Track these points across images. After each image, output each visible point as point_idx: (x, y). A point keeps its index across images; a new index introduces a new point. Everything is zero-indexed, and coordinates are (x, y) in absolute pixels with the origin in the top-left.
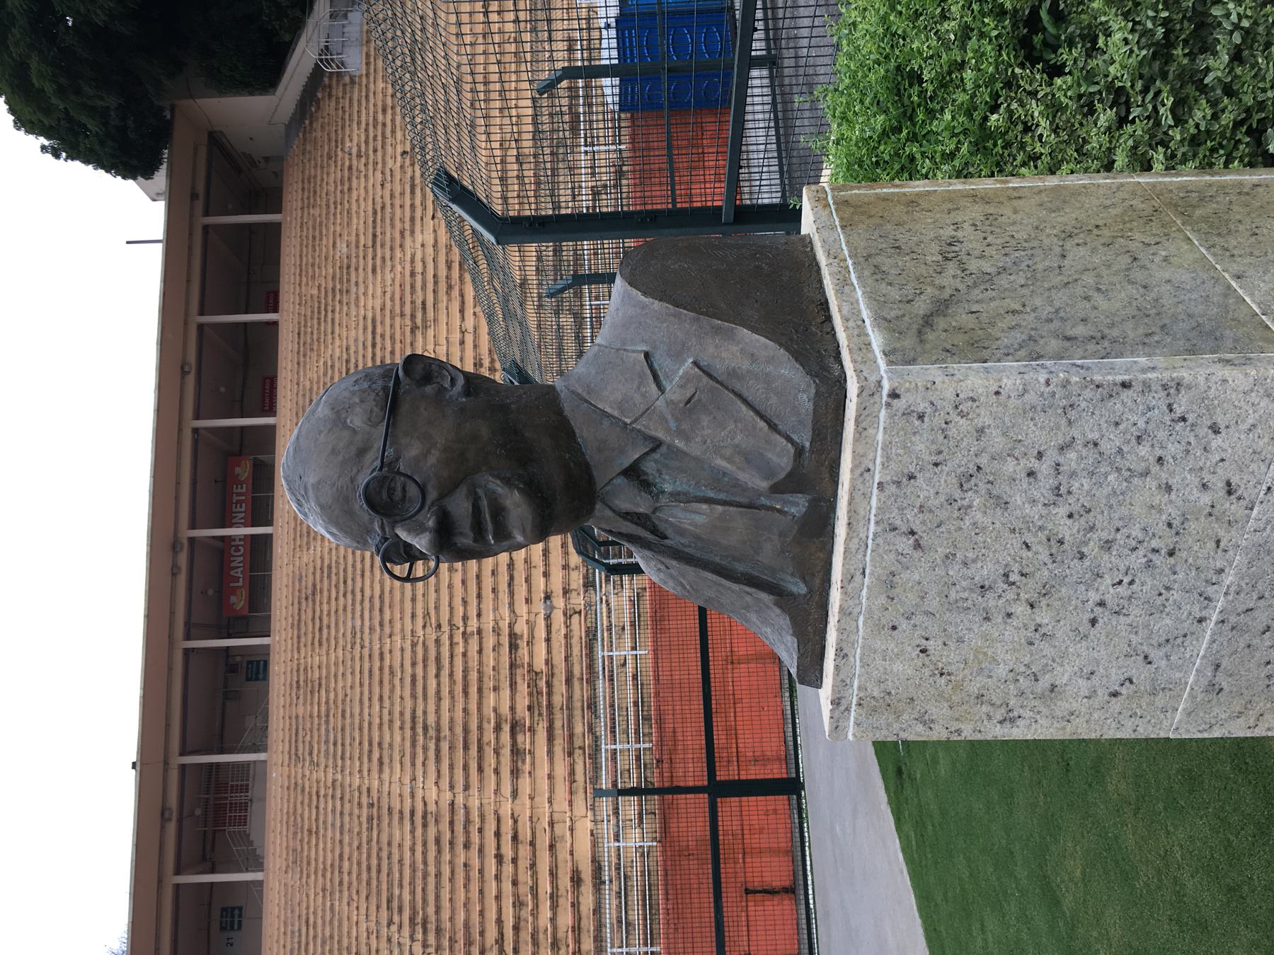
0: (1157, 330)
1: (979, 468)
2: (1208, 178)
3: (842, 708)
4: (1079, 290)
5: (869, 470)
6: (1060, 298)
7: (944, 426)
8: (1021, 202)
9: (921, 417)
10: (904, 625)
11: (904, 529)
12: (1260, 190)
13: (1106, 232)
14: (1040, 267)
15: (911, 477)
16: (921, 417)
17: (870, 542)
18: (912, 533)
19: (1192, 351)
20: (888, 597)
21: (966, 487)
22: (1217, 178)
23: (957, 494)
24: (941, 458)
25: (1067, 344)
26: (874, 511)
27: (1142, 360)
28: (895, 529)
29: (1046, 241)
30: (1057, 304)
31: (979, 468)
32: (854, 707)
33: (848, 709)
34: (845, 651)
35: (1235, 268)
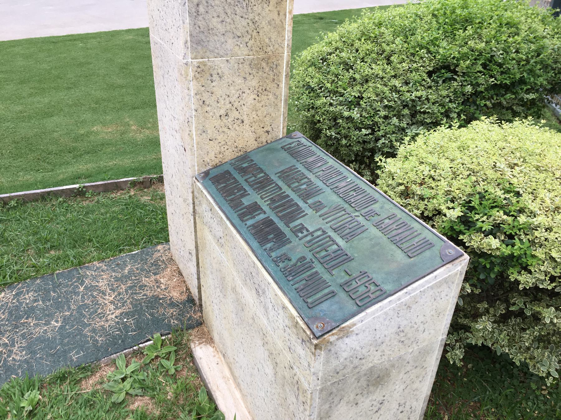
0: (202, 30)
2: (284, 74)
4: (223, 15)
6: (220, 10)
8: (276, 13)
12: (276, 86)
13: (255, 33)
14: (236, 8)
19: (191, 35)
22: (284, 76)
25: (195, 4)
27: (187, 21)
29: (251, 15)
30: (216, 7)
35: (232, 62)
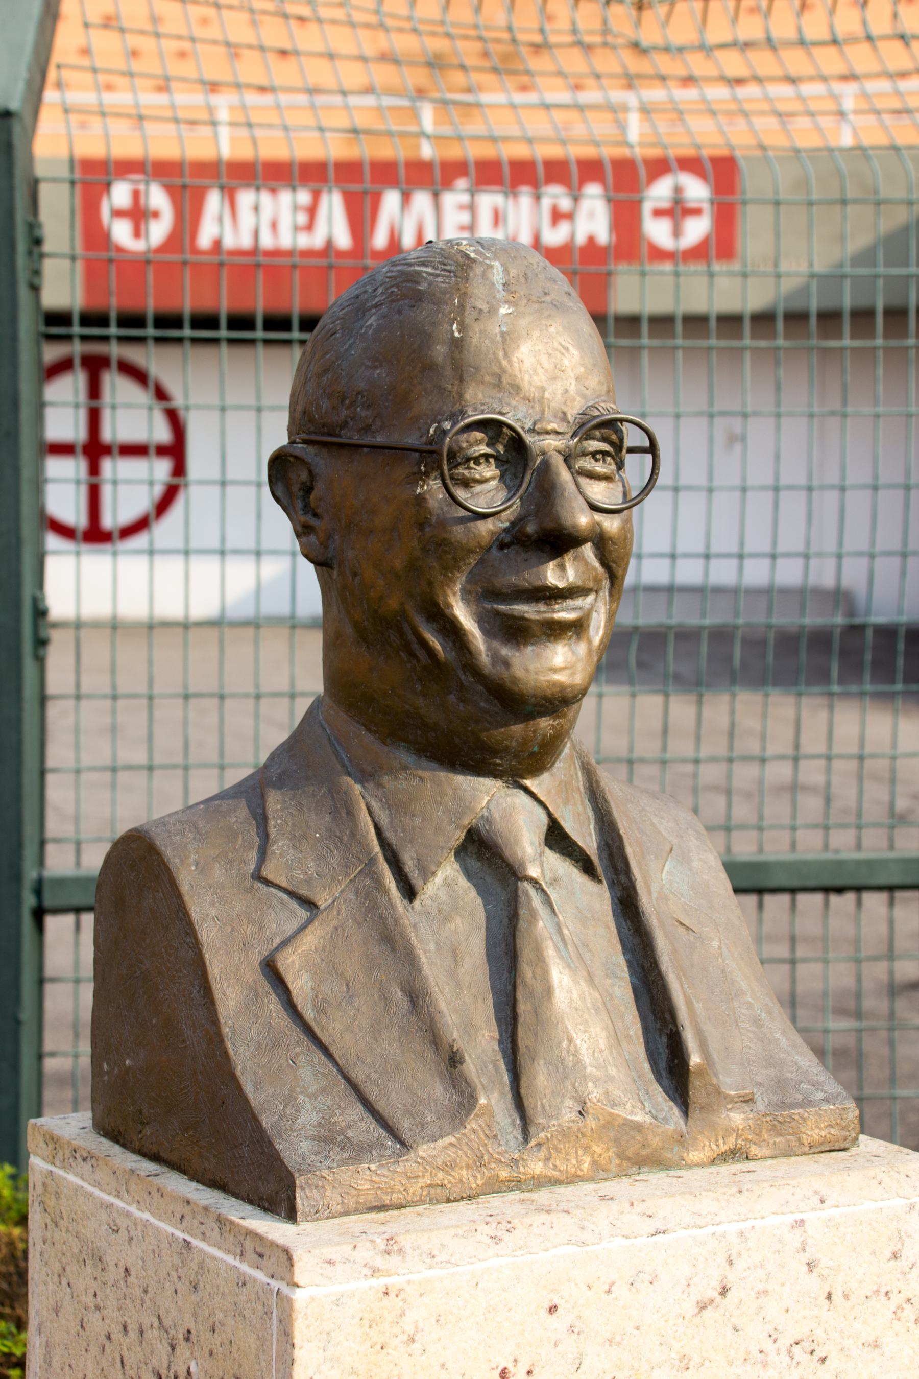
1: (823, 1360)
3: (379, 1262)
5: (822, 1201)
7: (883, 1291)
9: (895, 1256)
10: (558, 1323)
11: (732, 1277)
15: (811, 1266)
16: (895, 1256)
17: (710, 1229)
18: (724, 1291)
20: (612, 1284)
21: (796, 1350)
23: (785, 1341)
24: (837, 1297)
26: (758, 1223)
28: (731, 1263)
31: (823, 1360)
32: (380, 1282)
33: (375, 1271)
34: (507, 1237)
